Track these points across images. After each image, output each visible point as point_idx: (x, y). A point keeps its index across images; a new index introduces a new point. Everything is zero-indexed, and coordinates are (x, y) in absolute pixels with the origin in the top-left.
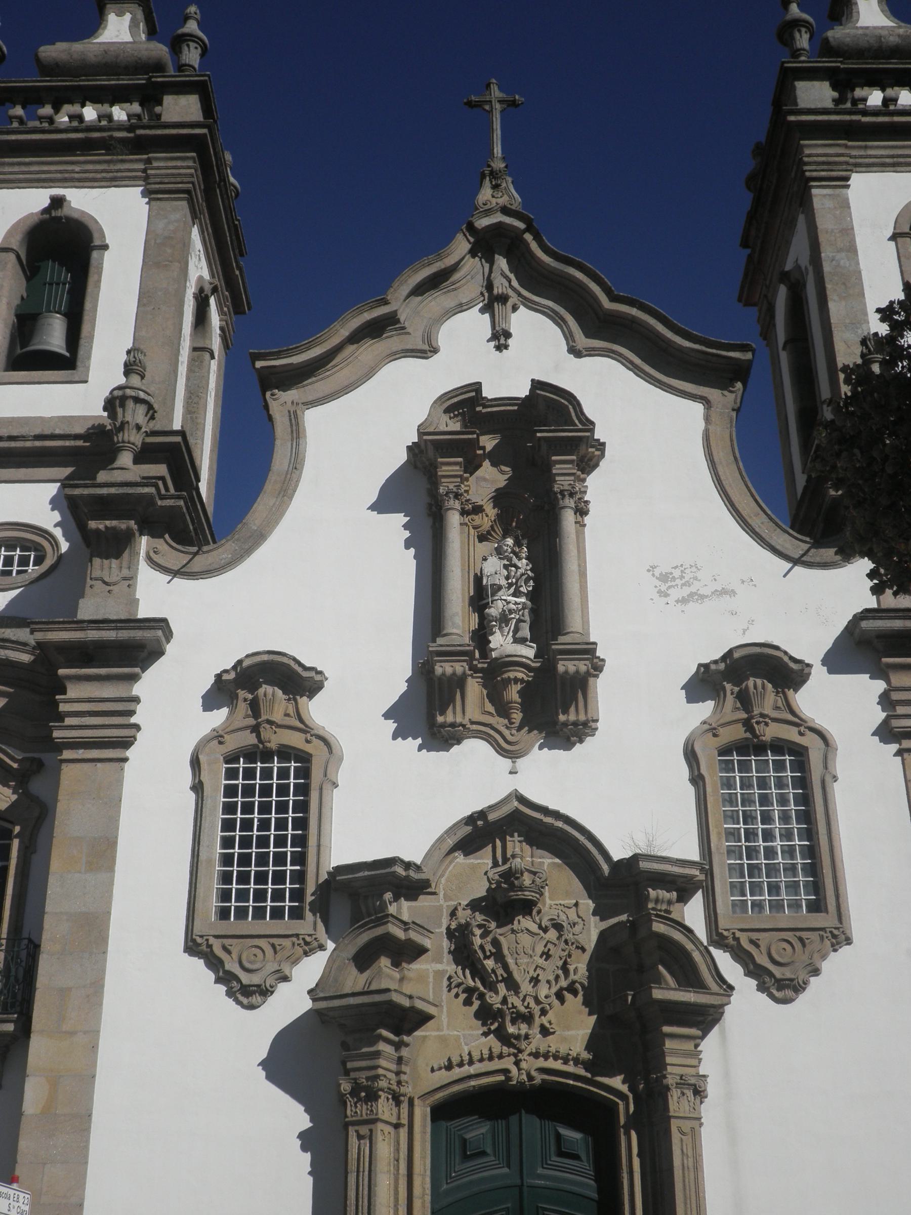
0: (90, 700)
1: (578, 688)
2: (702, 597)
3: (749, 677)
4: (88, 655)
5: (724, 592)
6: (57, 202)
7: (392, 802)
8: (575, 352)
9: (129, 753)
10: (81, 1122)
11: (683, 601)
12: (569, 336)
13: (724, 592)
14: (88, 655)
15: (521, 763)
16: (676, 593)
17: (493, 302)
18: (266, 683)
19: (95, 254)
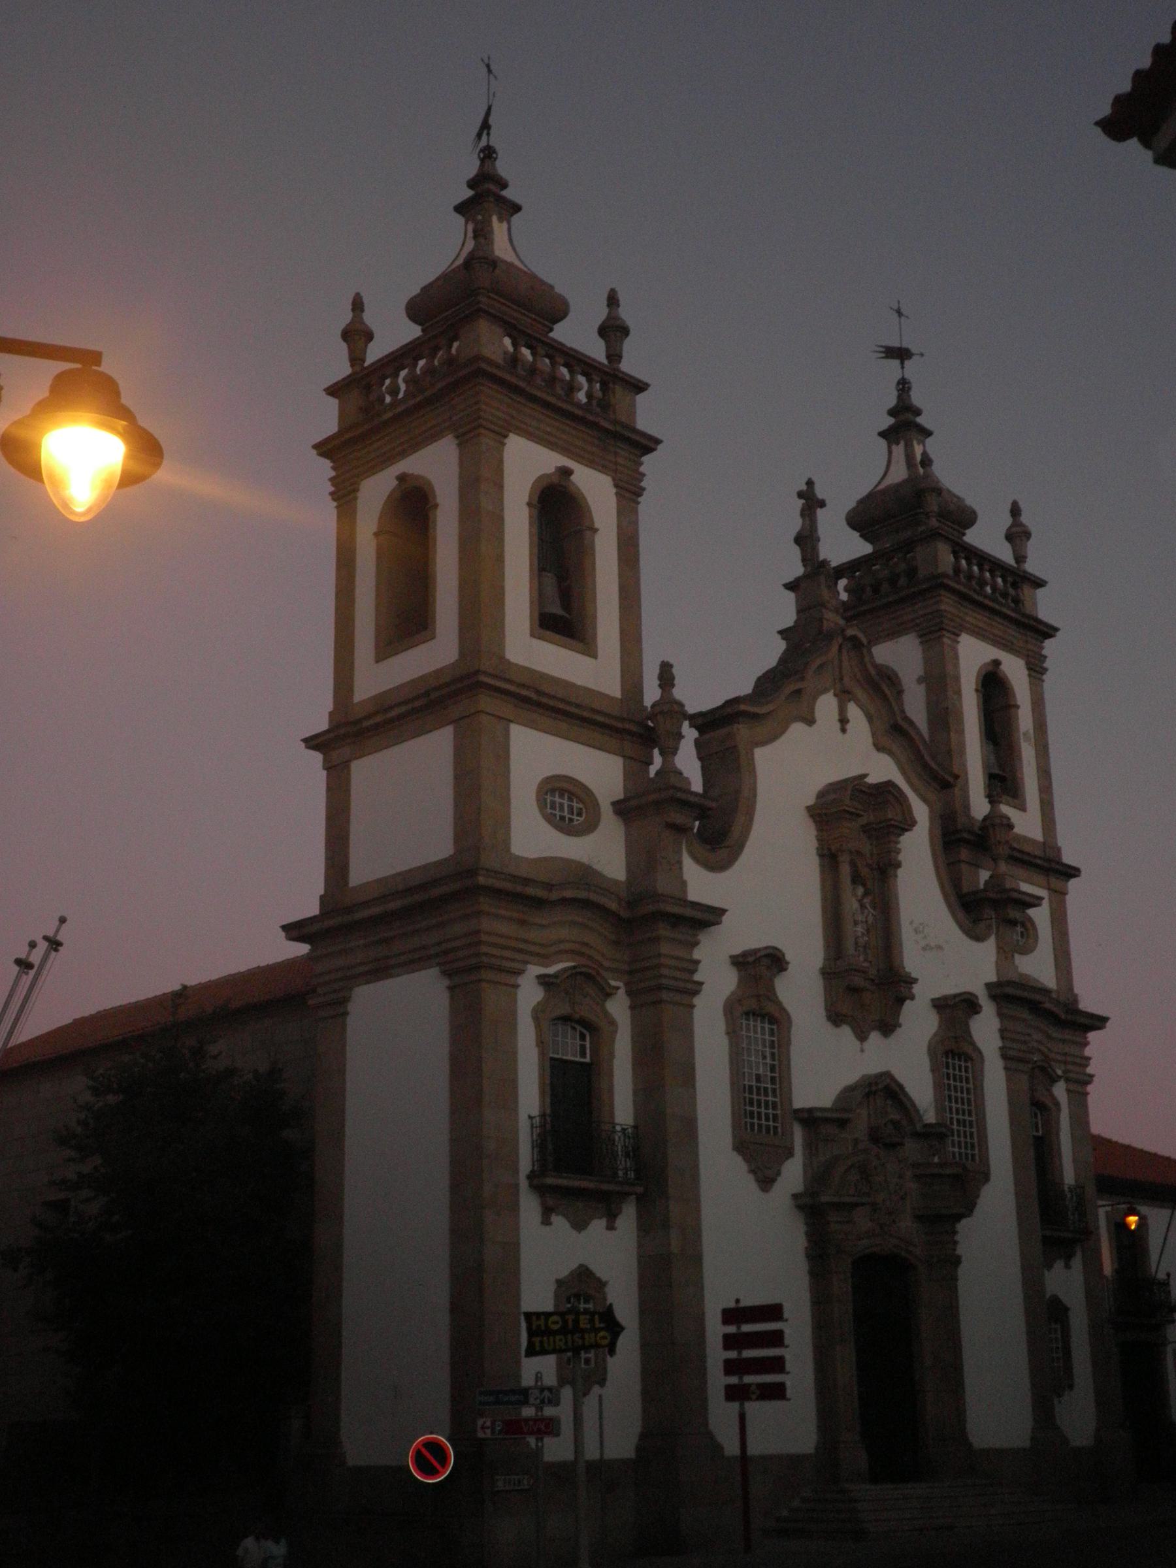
0: (677, 958)
1: (901, 1001)
2: (931, 948)
3: (956, 1009)
4: (676, 921)
5: (939, 947)
6: (566, 472)
7: (825, 1064)
8: (879, 748)
9: (697, 1001)
10: (698, 1259)
11: (924, 949)
12: (874, 735)
13: (939, 947)
14: (676, 921)
15: (866, 1045)
16: (923, 943)
17: (844, 696)
18: (761, 967)
19: (588, 533)
